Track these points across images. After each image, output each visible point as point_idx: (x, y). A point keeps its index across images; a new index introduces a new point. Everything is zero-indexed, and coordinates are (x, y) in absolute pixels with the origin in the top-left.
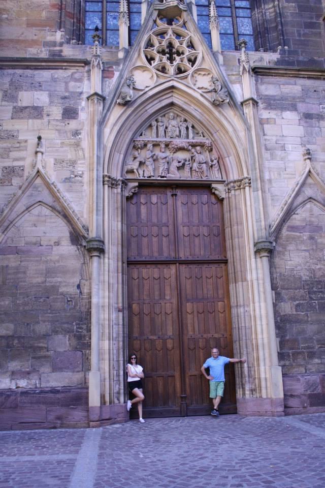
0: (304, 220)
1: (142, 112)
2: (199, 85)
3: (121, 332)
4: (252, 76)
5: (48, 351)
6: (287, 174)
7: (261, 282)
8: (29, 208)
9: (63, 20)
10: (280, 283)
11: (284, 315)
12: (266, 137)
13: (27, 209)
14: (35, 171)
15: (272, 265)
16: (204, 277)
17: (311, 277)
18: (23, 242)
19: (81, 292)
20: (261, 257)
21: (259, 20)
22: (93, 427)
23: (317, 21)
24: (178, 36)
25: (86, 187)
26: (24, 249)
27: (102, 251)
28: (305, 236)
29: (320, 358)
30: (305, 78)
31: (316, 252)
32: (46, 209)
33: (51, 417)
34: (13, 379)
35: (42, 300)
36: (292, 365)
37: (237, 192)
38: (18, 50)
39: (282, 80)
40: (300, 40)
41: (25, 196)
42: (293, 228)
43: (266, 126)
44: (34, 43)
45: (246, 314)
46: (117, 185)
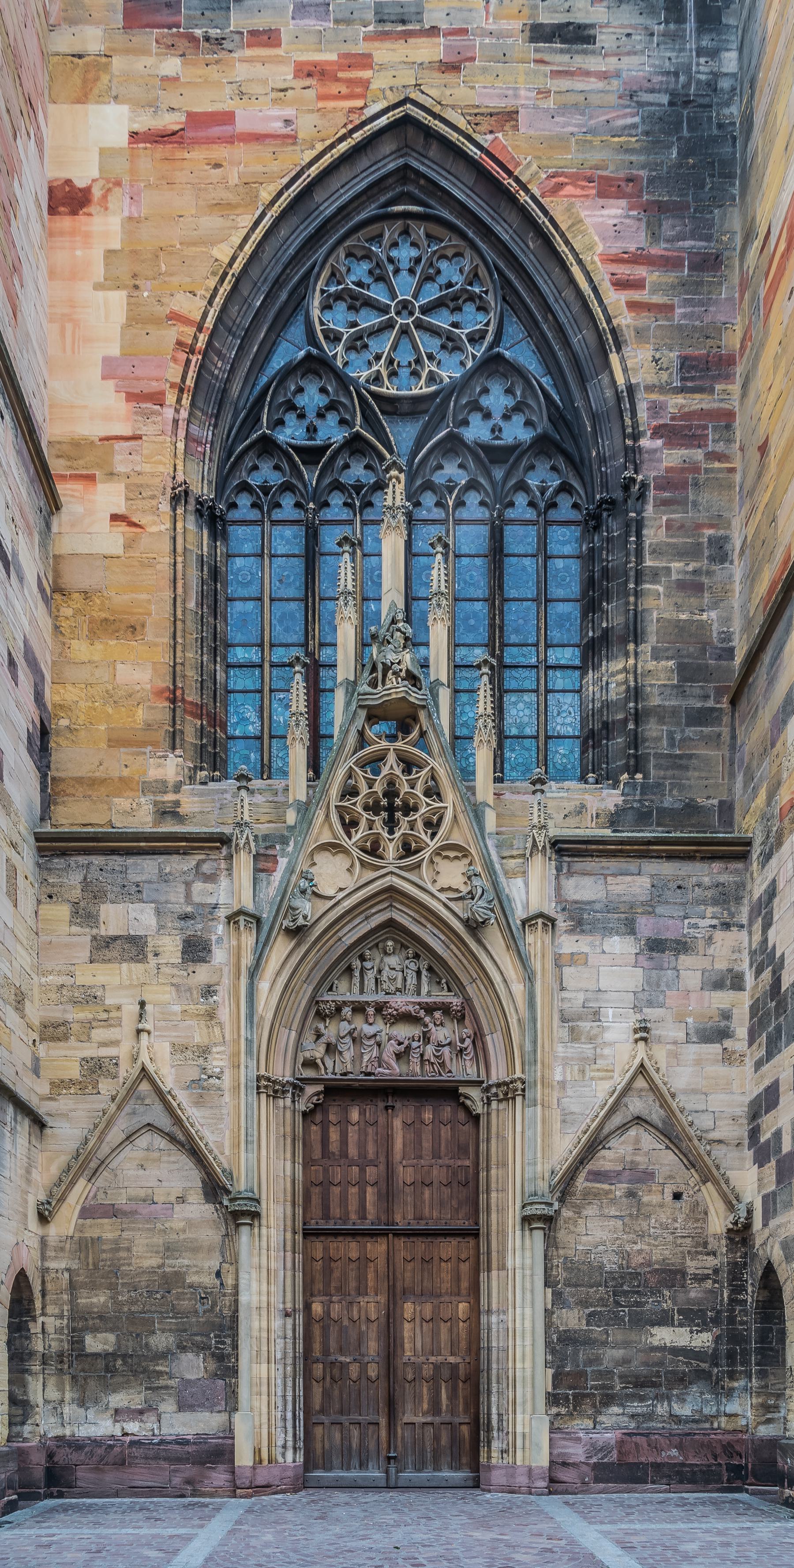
0: (622, 1160)
1: (331, 942)
2: (443, 882)
3: (290, 1351)
4: (550, 859)
5: (170, 1378)
6: (598, 1070)
7: (528, 1272)
8: (130, 1136)
9: (178, 727)
10: (560, 1274)
11: (565, 1331)
12: (564, 994)
13: (128, 1138)
14: (138, 1066)
15: (551, 1242)
16: (436, 1259)
17: (621, 1266)
18: (124, 1195)
19: (222, 1284)
20: (531, 1230)
21: (593, 700)
22: (241, 1497)
23: (718, 706)
24: (409, 764)
25: (227, 1098)
26: (126, 1208)
27: (256, 1215)
28: (620, 1189)
29: (623, 1406)
30: (662, 857)
31: (637, 1220)
32: (160, 1139)
33: (177, 1481)
34: (118, 1421)
35: (158, 1296)
36: (572, 1414)
37: (502, 1106)
38: (95, 803)
39: (613, 864)
40: (670, 756)
41: (123, 1113)
42: (598, 1176)
43: (566, 970)
44: (124, 784)
45: (501, 1326)
46: (284, 1092)
